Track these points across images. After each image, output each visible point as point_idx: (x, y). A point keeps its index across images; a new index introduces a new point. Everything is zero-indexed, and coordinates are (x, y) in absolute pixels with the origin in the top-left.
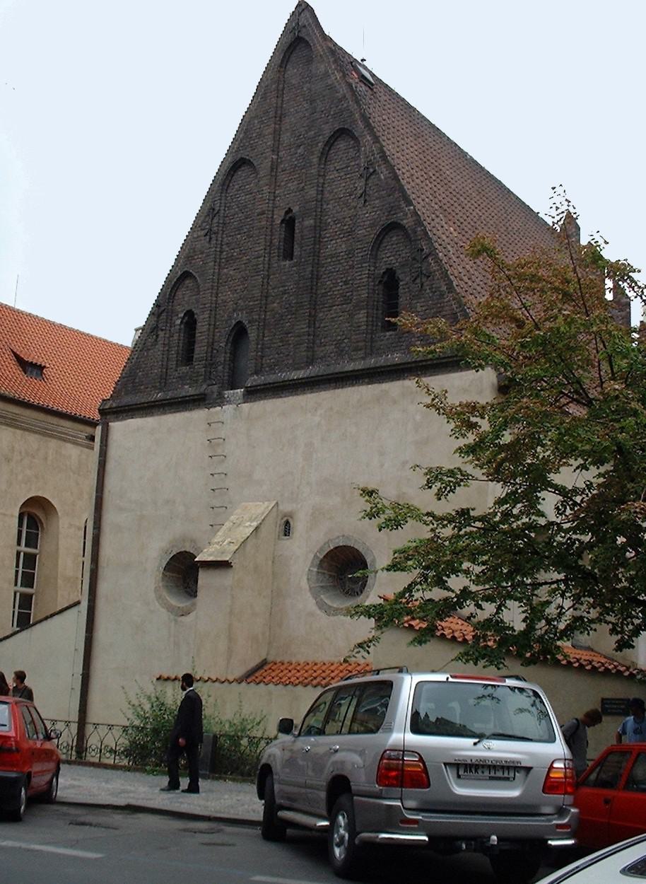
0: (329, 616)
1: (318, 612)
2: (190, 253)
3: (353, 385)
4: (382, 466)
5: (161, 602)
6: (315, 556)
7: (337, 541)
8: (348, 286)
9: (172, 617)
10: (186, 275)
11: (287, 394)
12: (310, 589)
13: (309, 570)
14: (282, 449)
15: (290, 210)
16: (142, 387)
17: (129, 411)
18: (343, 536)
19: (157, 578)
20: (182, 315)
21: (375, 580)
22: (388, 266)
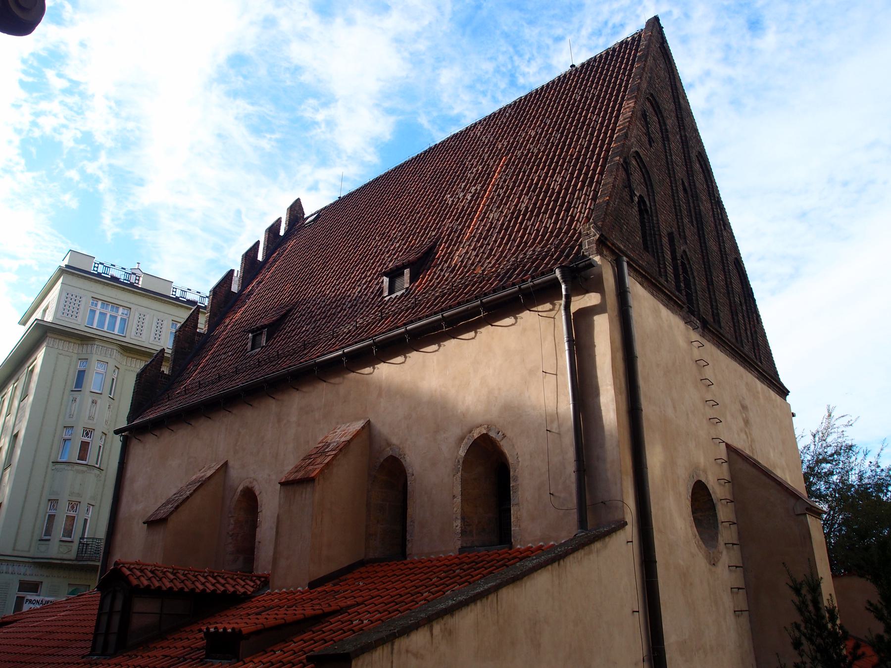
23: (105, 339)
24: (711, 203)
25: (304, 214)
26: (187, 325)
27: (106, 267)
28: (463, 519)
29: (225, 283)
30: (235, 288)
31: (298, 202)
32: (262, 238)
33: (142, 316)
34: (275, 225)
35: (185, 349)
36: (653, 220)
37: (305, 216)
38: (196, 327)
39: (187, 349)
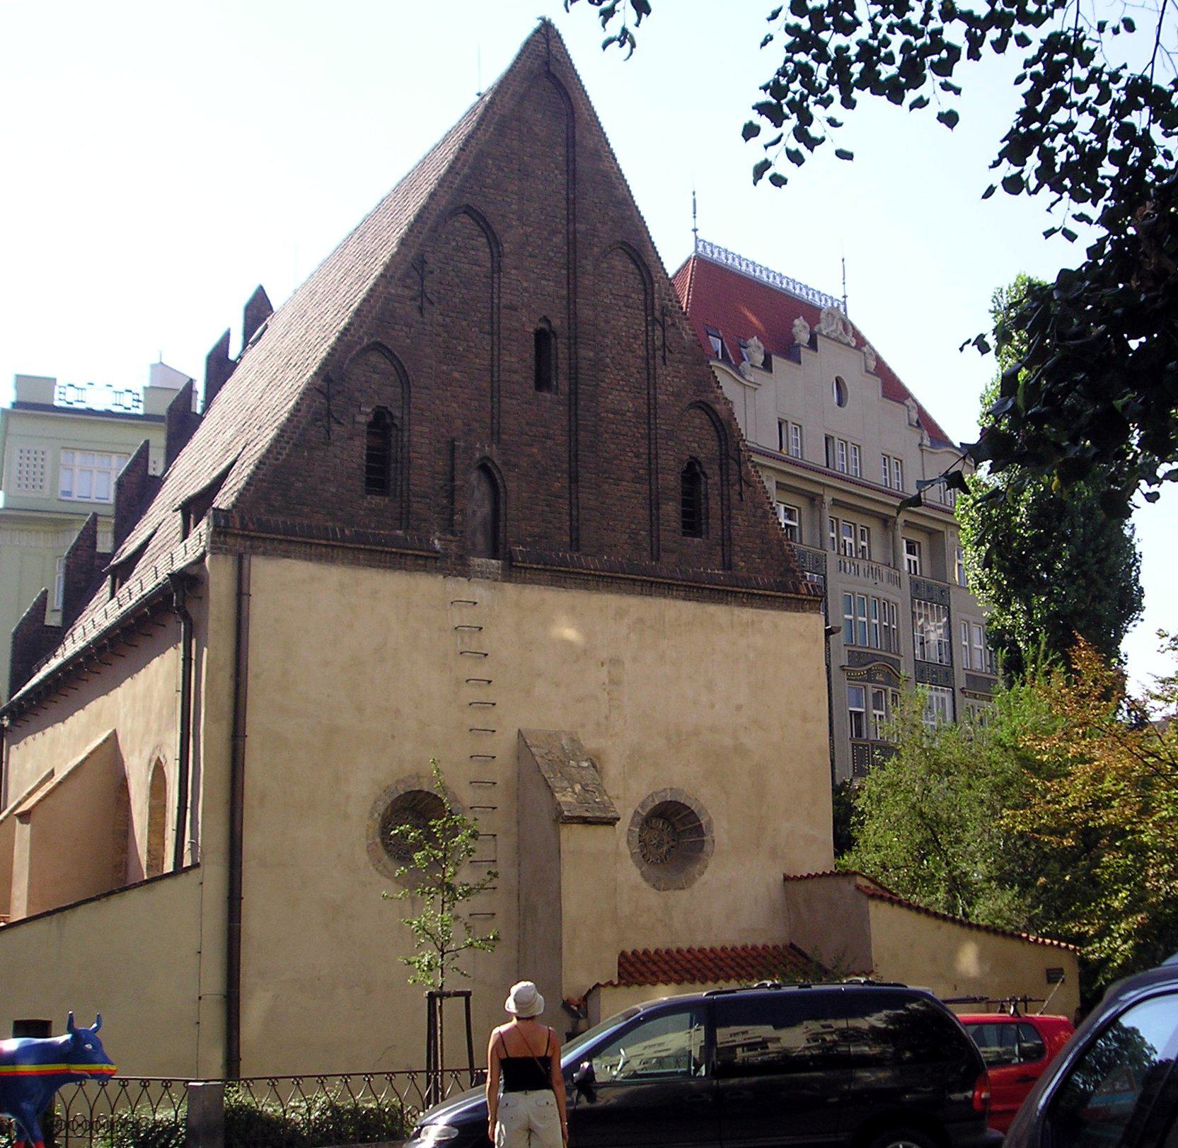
0: (659, 890)
1: (644, 885)
4: (713, 706)
5: (380, 868)
6: (636, 812)
7: (663, 794)
10: (378, 347)
11: (573, 586)
12: (632, 854)
13: (629, 830)
20: (369, 410)
24: (647, 320)
36: (402, 437)
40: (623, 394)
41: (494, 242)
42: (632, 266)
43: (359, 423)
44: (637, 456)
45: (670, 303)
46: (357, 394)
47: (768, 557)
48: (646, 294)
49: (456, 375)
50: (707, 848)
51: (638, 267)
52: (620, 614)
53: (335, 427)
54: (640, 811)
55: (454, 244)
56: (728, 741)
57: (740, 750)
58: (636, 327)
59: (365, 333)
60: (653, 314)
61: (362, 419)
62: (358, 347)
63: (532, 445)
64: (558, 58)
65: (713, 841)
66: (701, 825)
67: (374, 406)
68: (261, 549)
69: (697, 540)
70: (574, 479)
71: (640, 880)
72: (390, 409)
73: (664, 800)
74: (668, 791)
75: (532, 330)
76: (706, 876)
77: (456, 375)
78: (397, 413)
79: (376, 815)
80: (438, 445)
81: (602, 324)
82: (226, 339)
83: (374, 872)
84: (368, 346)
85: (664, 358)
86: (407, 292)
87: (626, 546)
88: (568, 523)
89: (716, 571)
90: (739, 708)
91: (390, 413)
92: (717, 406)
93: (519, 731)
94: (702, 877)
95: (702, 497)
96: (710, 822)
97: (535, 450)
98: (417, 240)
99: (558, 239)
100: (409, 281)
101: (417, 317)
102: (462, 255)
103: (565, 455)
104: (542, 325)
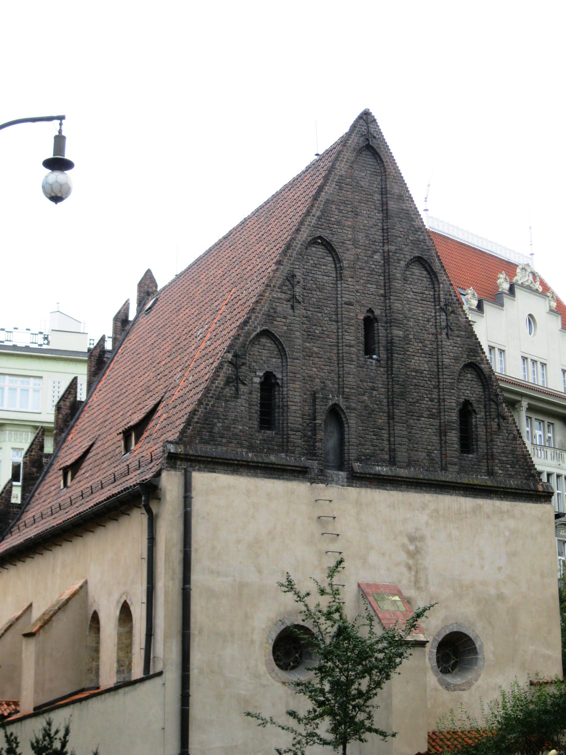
1: (440, 687)
2: (269, 311)
3: (451, 495)
4: (482, 567)
5: (274, 675)
7: (451, 627)
8: (433, 403)
9: (289, 691)
10: (266, 333)
11: (392, 488)
12: (432, 668)
13: (430, 651)
14: (395, 539)
15: (370, 311)
16: (224, 440)
17: (209, 462)
18: (456, 623)
19: (267, 650)
20: (262, 374)
21: (484, 662)
22: (467, 398)
23: (16, 422)
25: (156, 286)
26: (33, 449)
27: (8, 332)
28: (118, 661)
29: (69, 394)
30: (82, 395)
31: (148, 274)
32: (109, 332)
33: (57, 384)
34: (122, 311)
35: (34, 474)
37: (159, 289)
38: (42, 448)
39: (36, 474)
40: (421, 359)
41: (337, 259)
42: (425, 273)
43: (256, 383)
44: (432, 400)
45: (450, 297)
46: (253, 364)
47: (517, 466)
48: (435, 291)
49: (315, 349)
50: (480, 663)
51: (429, 273)
52: (424, 507)
53: (241, 386)
54: (437, 638)
55: (312, 262)
56: (493, 591)
57: (501, 597)
58: (428, 313)
59: (258, 324)
60: (439, 305)
61: (257, 380)
62: (255, 333)
63: (364, 395)
64: (375, 135)
65: (484, 658)
66: (475, 648)
67: (264, 372)
68: (197, 468)
69: (470, 456)
70: (391, 417)
71: (437, 684)
72: (275, 373)
73: (451, 631)
74: (455, 625)
75: (362, 318)
76: (480, 682)
77: (315, 349)
78: (279, 376)
79: (270, 641)
80: (305, 396)
81: (407, 312)
82: (126, 307)
83: (270, 678)
84: (261, 332)
85: (447, 334)
86: (283, 296)
87: (425, 461)
88: (388, 446)
89: (484, 477)
90: (500, 569)
91: (274, 376)
92: (483, 366)
93: (359, 585)
94: (477, 682)
95: (473, 427)
96: (481, 646)
97: (365, 398)
98: (289, 261)
99: (377, 257)
100: (284, 288)
101: (291, 311)
102: (317, 269)
103: (385, 401)
104: (369, 315)
